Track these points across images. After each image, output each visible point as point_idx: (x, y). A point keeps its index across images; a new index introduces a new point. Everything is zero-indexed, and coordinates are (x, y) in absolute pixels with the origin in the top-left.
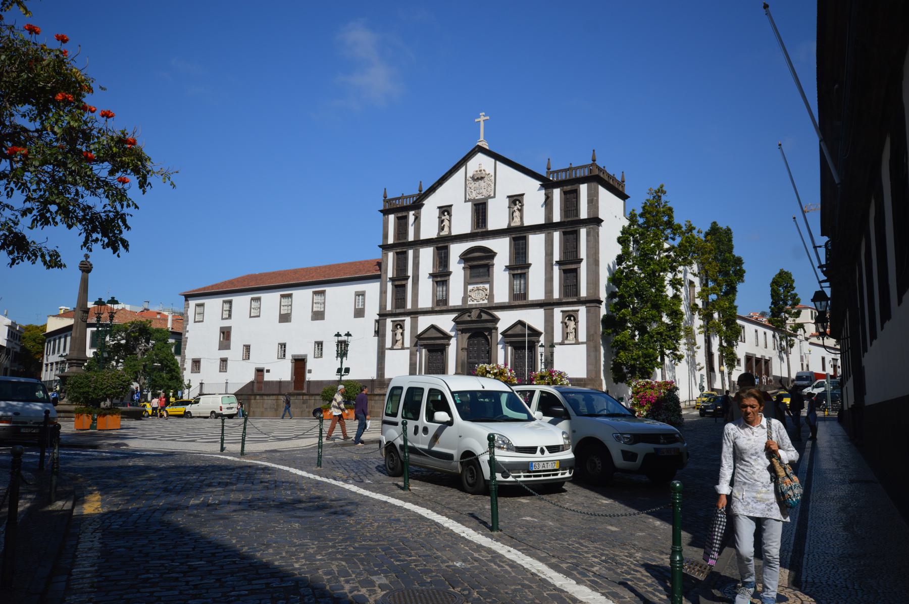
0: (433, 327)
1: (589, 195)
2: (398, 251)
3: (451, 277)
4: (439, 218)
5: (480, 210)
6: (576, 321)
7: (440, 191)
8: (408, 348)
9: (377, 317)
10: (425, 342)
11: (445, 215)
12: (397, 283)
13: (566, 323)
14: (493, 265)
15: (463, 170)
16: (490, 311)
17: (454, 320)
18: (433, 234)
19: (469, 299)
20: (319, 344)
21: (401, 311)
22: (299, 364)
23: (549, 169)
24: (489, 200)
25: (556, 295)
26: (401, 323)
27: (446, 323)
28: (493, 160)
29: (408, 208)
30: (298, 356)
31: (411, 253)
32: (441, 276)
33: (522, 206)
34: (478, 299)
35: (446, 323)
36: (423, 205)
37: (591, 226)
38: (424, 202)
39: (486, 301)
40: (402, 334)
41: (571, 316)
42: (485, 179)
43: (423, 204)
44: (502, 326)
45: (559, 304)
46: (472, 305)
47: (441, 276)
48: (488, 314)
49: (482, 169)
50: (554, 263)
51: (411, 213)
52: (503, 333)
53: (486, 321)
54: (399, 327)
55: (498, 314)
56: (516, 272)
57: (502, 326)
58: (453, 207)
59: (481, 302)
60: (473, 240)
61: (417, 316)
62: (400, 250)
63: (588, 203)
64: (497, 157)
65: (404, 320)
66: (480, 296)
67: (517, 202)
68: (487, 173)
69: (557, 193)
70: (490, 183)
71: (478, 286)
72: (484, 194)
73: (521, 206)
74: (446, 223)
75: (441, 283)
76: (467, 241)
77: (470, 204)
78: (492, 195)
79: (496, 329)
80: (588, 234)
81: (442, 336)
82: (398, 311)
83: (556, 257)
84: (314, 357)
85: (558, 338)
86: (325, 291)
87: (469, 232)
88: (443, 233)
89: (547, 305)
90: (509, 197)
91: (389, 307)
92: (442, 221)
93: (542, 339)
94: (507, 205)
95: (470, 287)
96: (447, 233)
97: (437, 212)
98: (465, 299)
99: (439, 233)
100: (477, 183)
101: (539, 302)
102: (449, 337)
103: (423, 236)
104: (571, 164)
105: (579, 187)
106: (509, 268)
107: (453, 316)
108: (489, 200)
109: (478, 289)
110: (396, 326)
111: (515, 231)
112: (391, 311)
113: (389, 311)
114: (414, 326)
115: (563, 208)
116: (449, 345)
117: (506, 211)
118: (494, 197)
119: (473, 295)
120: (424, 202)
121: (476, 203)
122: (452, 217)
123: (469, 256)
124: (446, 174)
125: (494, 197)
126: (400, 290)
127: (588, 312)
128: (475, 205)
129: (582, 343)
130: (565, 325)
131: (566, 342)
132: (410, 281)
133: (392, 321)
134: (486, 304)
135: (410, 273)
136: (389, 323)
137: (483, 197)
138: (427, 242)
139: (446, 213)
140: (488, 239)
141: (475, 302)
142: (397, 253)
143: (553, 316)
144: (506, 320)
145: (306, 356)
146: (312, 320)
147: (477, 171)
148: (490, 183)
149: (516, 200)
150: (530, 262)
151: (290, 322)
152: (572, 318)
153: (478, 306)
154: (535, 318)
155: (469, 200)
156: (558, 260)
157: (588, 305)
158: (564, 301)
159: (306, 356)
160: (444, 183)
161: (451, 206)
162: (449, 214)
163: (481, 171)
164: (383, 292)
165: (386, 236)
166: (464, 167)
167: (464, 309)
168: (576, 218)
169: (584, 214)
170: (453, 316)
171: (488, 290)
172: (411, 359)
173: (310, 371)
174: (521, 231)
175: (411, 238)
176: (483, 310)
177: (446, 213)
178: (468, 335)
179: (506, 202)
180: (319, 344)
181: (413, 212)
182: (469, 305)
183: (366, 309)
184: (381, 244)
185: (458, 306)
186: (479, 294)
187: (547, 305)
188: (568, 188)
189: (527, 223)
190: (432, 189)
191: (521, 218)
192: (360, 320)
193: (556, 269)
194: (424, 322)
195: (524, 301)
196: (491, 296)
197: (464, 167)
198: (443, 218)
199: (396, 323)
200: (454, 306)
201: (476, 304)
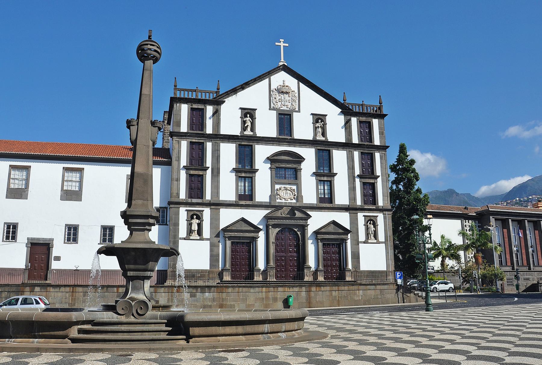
2: (194, 141)
3: (257, 174)
6: (375, 225)
7: (241, 94)
10: (233, 234)
12: (192, 172)
13: (368, 226)
16: (304, 210)
21: (199, 201)
25: (359, 202)
31: (209, 146)
39: (294, 201)
40: (200, 225)
41: (371, 221)
45: (362, 209)
54: (195, 217)
56: (322, 179)
59: (289, 201)
60: (279, 145)
62: (197, 141)
65: (203, 211)
68: (293, 90)
71: (286, 186)
72: (289, 107)
75: (243, 179)
76: (273, 144)
77: (274, 113)
78: (297, 109)
80: (381, 158)
81: (252, 229)
82: (194, 201)
85: (362, 237)
88: (248, 132)
89: (351, 209)
91: (183, 195)
95: (277, 187)
103: (223, 131)
106: (315, 174)
110: (192, 218)
114: (215, 220)
118: (299, 111)
119: (281, 193)
123: (275, 158)
124: (251, 80)
125: (299, 111)
127: (385, 218)
129: (382, 243)
130: (367, 229)
131: (369, 241)
132: (209, 172)
133: (187, 210)
135: (209, 163)
136: (183, 212)
137: (288, 109)
139: (248, 115)
141: (283, 201)
154: (344, 219)
155: (274, 109)
158: (365, 207)
162: (253, 117)
166: (267, 80)
169: (377, 142)
174: (326, 145)
175: (209, 130)
176: (293, 209)
177: (248, 115)
178: (278, 230)
179: (311, 119)
187: (351, 209)
188: (363, 119)
190: (234, 91)
191: (324, 134)
193: (357, 180)
196: (299, 197)
199: (192, 213)
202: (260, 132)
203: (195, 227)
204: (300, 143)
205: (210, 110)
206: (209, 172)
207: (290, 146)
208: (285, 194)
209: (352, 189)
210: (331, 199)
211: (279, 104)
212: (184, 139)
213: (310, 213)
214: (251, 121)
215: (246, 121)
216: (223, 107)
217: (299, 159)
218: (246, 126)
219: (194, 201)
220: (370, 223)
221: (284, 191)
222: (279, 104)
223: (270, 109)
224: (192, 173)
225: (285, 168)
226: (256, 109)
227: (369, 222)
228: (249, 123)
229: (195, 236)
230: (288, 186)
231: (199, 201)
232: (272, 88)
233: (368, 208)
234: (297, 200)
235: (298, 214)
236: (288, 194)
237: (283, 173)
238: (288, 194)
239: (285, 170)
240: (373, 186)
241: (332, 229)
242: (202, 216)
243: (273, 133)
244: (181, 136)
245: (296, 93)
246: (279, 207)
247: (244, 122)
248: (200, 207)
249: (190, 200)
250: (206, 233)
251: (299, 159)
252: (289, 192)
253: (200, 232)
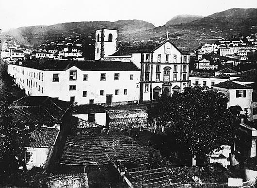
5: (167, 56)
20: (117, 91)
22: (109, 98)
27: (160, 85)
32: (158, 73)
34: (167, 79)
35: (160, 85)
40: (148, 88)
44: (173, 87)
45: (183, 81)
47: (158, 73)
48: (170, 83)
51: (151, 54)
57: (173, 87)
88: (159, 61)
89: (180, 82)
107: (163, 83)
126: (147, 75)
138: (155, 63)
144: (174, 85)
149: (175, 56)
170: (163, 83)
180: (117, 91)
187: (180, 82)
194: (154, 85)
203: (146, 89)
229: (146, 91)
246: (166, 82)
250: (149, 91)
253: (148, 90)
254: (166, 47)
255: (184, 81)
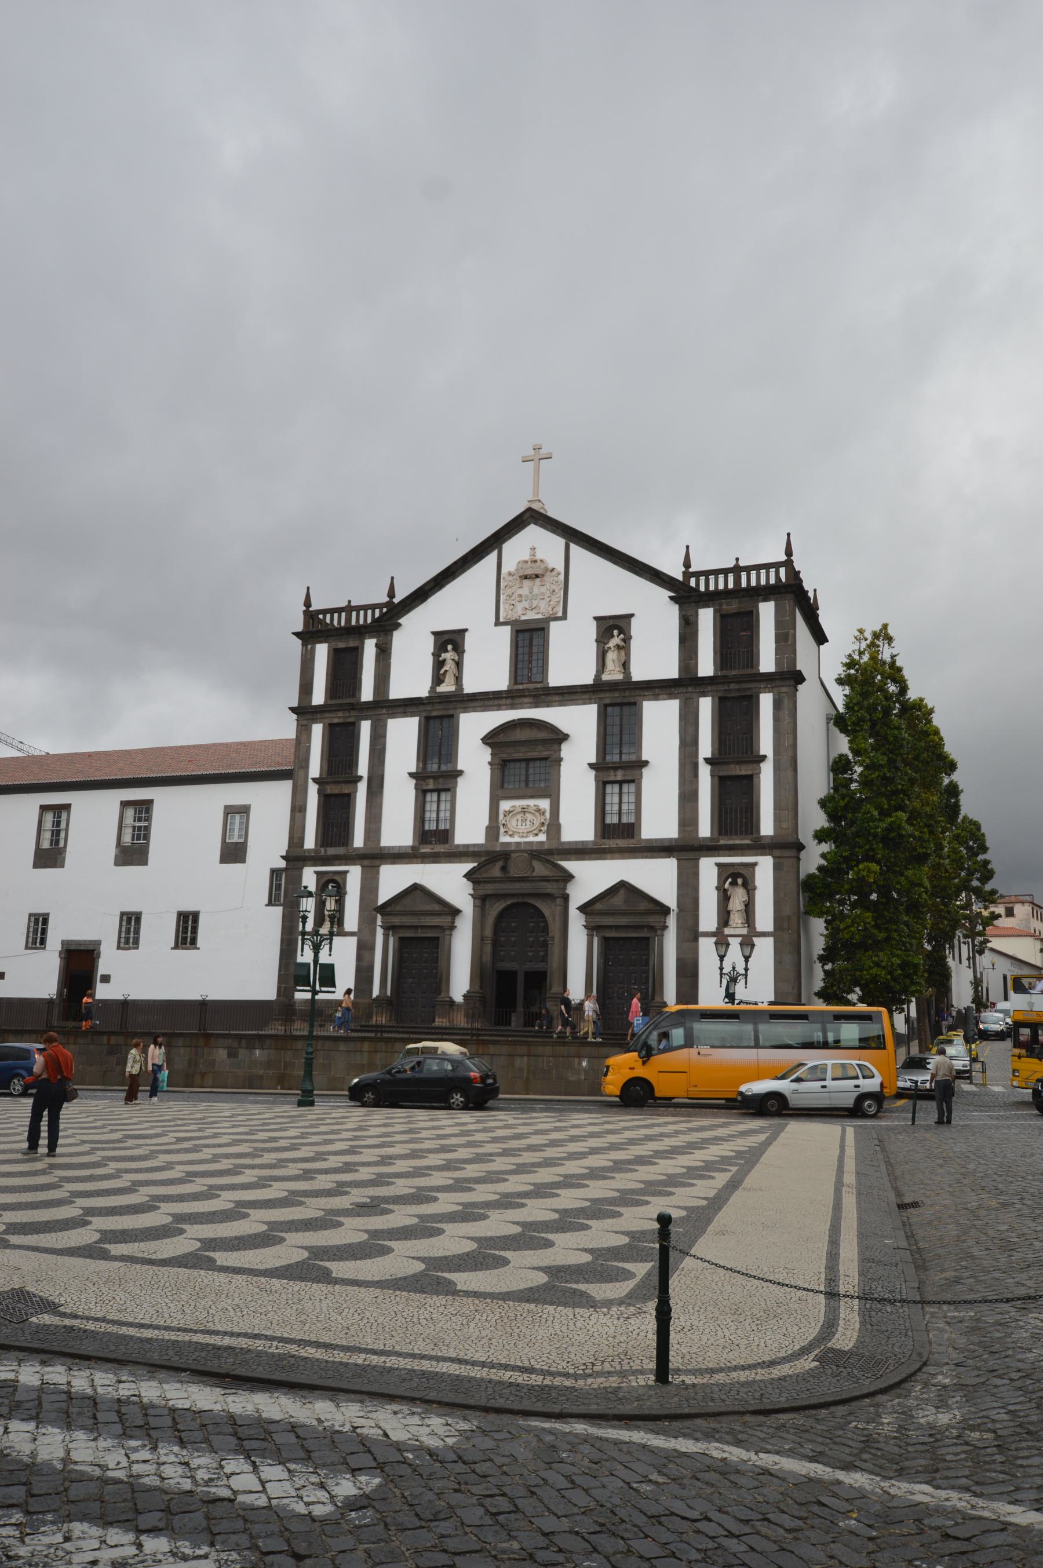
0: (416, 890)
1: (779, 624)
2: (336, 721)
4: (436, 655)
8: (352, 934)
9: (283, 864)
11: (446, 651)
12: (330, 789)
13: (725, 891)
14: (560, 760)
15: (492, 558)
16: (549, 858)
17: (468, 876)
18: (421, 688)
19: (502, 830)
21: (340, 851)
23: (687, 564)
24: (552, 624)
25: (705, 829)
26: (337, 878)
28: (561, 542)
29: (362, 632)
30: (78, 942)
31: (365, 728)
33: (627, 640)
36: (398, 626)
37: (784, 689)
38: (400, 621)
39: (542, 837)
42: (545, 578)
43: (399, 625)
44: (581, 893)
45: (709, 848)
46: (509, 844)
49: (538, 557)
50: (701, 761)
52: (583, 909)
53: (545, 879)
55: (570, 866)
57: (581, 893)
58: (467, 634)
59: (531, 839)
60: (513, 707)
61: (376, 862)
63: (776, 642)
64: (572, 535)
65: (346, 872)
66: (528, 827)
67: (616, 632)
68: (550, 566)
69: (706, 618)
70: (553, 587)
73: (624, 640)
74: (450, 666)
76: (499, 708)
77: (506, 631)
78: (560, 614)
79: (566, 898)
80: (777, 705)
83: (705, 748)
84: (119, 948)
85: (708, 918)
86: (150, 802)
87: (505, 688)
88: (447, 687)
90: (596, 618)
91: (310, 842)
92: (442, 663)
93: (672, 921)
94: (594, 636)
95: (505, 805)
96: (453, 688)
97: (429, 644)
98: (493, 830)
99: (433, 689)
100: (525, 591)
101: (666, 844)
102: (455, 912)
103: (397, 691)
104: (737, 559)
105: (757, 608)
107: (469, 866)
108: (552, 624)
109: (524, 810)
111: (610, 691)
112: (315, 850)
113: (309, 850)
114: (370, 886)
115: (718, 650)
116: (452, 927)
117: (594, 646)
118: (564, 617)
119: (513, 824)
120: (400, 621)
121: (519, 628)
122: (466, 655)
123: (501, 738)
125: (564, 617)
127: (777, 868)
128: (518, 632)
130: (724, 898)
132: (362, 789)
133: (316, 872)
134: (542, 843)
135: (363, 769)
136: (309, 878)
137: (540, 616)
138: (407, 706)
139: (450, 647)
140: (548, 705)
141: (516, 839)
142: (332, 726)
143: (696, 874)
145: (98, 943)
146: (116, 864)
147: (526, 562)
148: (553, 587)
150: (644, 758)
151: (63, 867)
152: (740, 881)
153: (522, 848)
156: (709, 755)
157: (777, 853)
158: (722, 842)
159: (98, 943)
160: (447, 583)
161: (462, 632)
162: (459, 649)
163: (535, 561)
164: (298, 809)
165: (306, 687)
167: (488, 853)
168: (754, 671)
171: (548, 815)
172: (359, 958)
173: (106, 979)
174: (625, 690)
176: (536, 854)
177: (450, 647)
179: (591, 631)
181: (374, 641)
182: (503, 844)
183: (249, 844)
184: (295, 704)
185: (475, 845)
186: (524, 820)
189: (638, 674)
191: (626, 665)
192: (233, 868)
193: (705, 773)
195: (632, 841)
196: (554, 827)
197: (495, 553)
198: (444, 656)
199: (325, 879)
200: (468, 846)
201: (518, 844)
202: (471, 685)
204: (562, 694)
205: (370, 647)
206: (362, 789)
207: (536, 705)
208: (520, 823)
209: (688, 797)
210: (630, 830)
211: (520, 607)
212: (315, 721)
213: (564, 864)
214: (456, 658)
215: (445, 660)
216: (397, 635)
217: (558, 737)
218: (442, 672)
219: (331, 851)
220: (734, 883)
221: (519, 817)
222: (520, 607)
223: (498, 623)
224: (329, 792)
225: (528, 761)
226: (466, 630)
227: (730, 880)
228: (450, 666)
230: (531, 802)
231: (340, 851)
232: (504, 570)
233: (731, 842)
234: (548, 833)
235: (540, 869)
236: (528, 823)
237: (523, 772)
238: (528, 823)
239: (527, 765)
240: (748, 784)
241: (618, 901)
242: (345, 883)
243: (500, 681)
244: (313, 713)
245: (559, 574)
247: (439, 664)
248: (340, 865)
249: (323, 850)
251: (558, 737)
252: (529, 816)
254: (509, 566)
255: (732, 850)
